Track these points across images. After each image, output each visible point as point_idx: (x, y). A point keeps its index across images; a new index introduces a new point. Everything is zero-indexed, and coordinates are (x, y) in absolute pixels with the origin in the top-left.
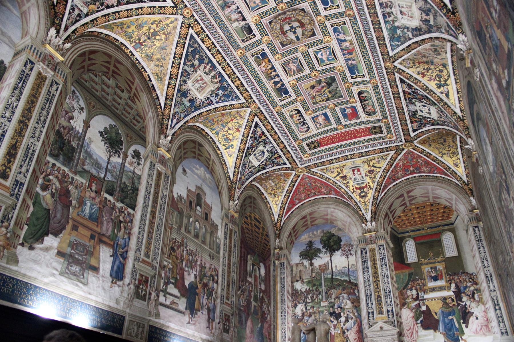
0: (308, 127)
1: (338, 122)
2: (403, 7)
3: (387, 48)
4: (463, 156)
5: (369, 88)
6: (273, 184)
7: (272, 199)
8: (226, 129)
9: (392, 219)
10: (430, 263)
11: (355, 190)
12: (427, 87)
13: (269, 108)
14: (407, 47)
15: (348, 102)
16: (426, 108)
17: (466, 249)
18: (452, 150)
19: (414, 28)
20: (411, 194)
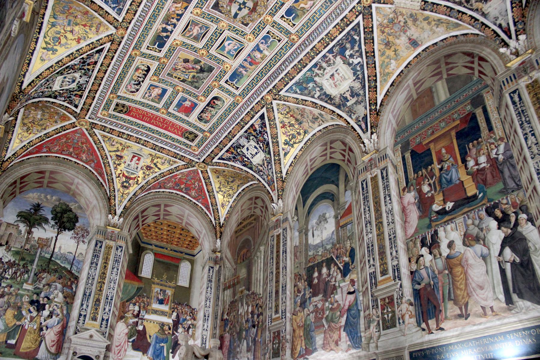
0: (137, 90)
1: (167, 105)
2: (338, 74)
3: (284, 87)
4: (234, 202)
5: (228, 100)
6: (39, 117)
7: (20, 131)
8: (69, 29)
9: (141, 224)
10: (161, 285)
11: (121, 175)
12: (277, 137)
13: (130, 46)
14: (302, 100)
15: (197, 97)
16: (256, 150)
17: (197, 284)
18: (231, 192)
19: (327, 93)
20: (168, 209)
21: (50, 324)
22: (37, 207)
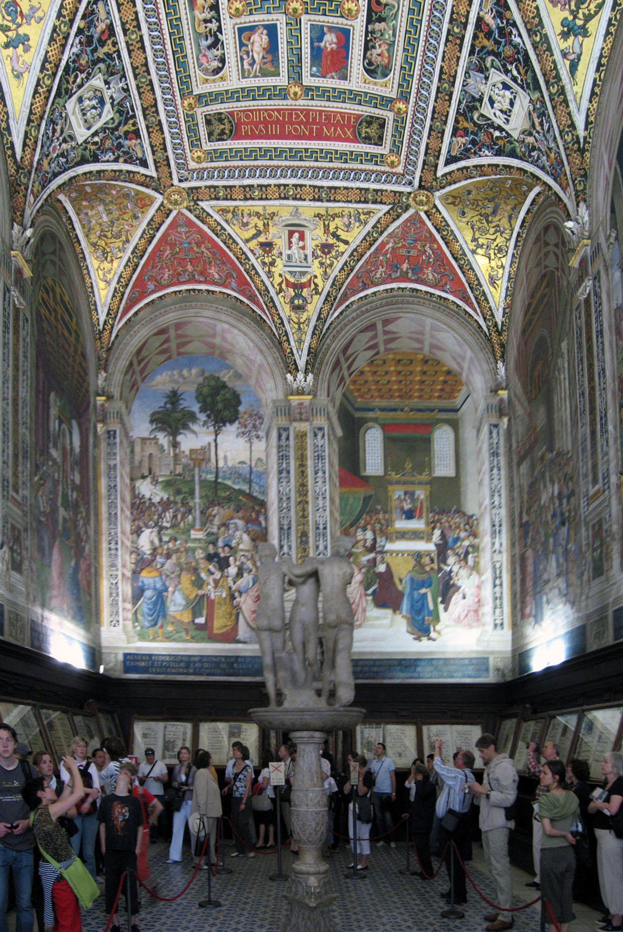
21: (242, 585)
22: (174, 397)
